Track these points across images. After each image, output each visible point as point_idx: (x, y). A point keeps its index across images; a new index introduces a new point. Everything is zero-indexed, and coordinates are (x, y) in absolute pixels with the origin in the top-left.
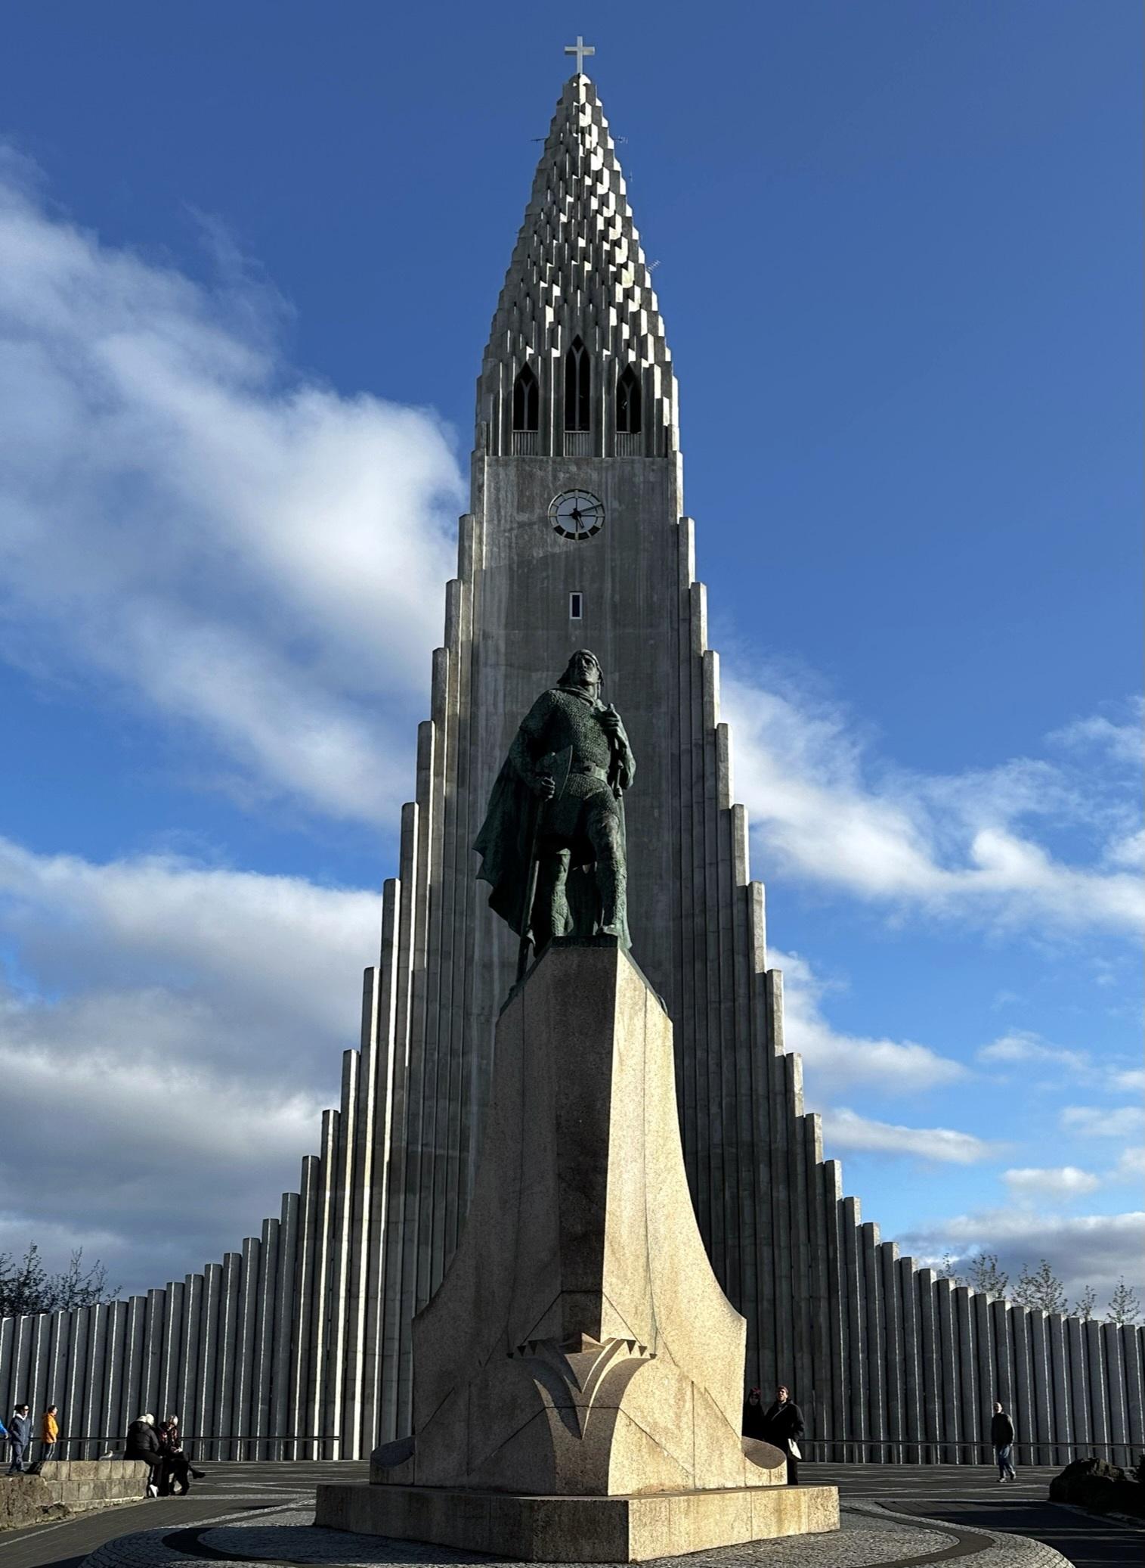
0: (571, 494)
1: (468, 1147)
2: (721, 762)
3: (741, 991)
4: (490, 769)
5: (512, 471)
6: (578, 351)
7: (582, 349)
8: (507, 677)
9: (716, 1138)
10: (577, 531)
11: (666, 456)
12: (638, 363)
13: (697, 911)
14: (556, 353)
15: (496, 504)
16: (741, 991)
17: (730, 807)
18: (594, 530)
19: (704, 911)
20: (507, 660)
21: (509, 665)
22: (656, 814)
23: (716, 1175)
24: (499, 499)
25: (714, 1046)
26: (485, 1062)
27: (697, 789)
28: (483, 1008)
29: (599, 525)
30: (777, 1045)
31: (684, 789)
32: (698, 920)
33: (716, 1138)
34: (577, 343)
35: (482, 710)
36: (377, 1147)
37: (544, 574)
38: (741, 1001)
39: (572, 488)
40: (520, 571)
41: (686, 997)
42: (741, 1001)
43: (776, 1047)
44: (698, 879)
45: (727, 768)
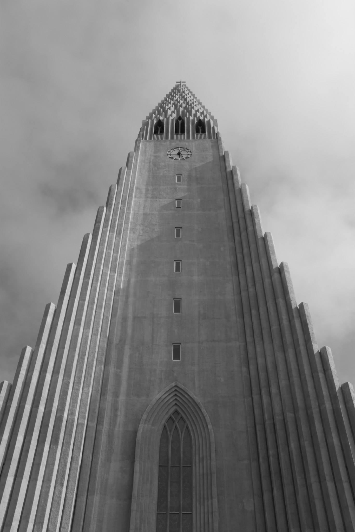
0: (177, 149)
1: (103, 422)
2: (256, 218)
3: (284, 317)
4: (134, 233)
5: (152, 144)
6: (180, 120)
7: (181, 120)
8: (145, 201)
9: (277, 409)
10: (179, 158)
11: (217, 138)
12: (204, 119)
13: (250, 284)
14: (171, 118)
15: (145, 152)
16: (284, 317)
17: (263, 236)
18: (188, 157)
19: (254, 285)
20: (146, 196)
21: (146, 197)
22: (222, 249)
23: (280, 433)
24: (146, 150)
25: (268, 353)
26: (119, 370)
27: (243, 234)
28: (120, 340)
29: (189, 156)
30: (314, 343)
31: (237, 238)
32: (251, 290)
33: (277, 409)
34: (180, 118)
35: (132, 212)
36: (34, 409)
37: (165, 170)
38: (285, 322)
39: (178, 147)
40: (153, 169)
41: (248, 331)
42: (285, 322)
43: (313, 344)
44: (248, 270)
45: (259, 221)
